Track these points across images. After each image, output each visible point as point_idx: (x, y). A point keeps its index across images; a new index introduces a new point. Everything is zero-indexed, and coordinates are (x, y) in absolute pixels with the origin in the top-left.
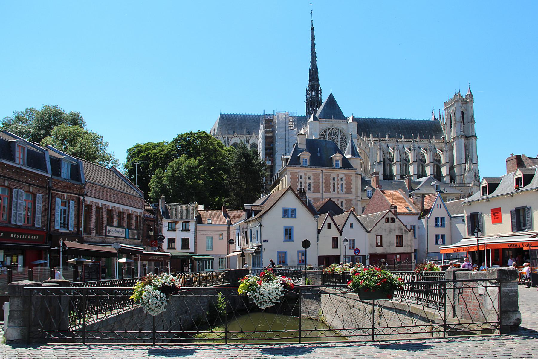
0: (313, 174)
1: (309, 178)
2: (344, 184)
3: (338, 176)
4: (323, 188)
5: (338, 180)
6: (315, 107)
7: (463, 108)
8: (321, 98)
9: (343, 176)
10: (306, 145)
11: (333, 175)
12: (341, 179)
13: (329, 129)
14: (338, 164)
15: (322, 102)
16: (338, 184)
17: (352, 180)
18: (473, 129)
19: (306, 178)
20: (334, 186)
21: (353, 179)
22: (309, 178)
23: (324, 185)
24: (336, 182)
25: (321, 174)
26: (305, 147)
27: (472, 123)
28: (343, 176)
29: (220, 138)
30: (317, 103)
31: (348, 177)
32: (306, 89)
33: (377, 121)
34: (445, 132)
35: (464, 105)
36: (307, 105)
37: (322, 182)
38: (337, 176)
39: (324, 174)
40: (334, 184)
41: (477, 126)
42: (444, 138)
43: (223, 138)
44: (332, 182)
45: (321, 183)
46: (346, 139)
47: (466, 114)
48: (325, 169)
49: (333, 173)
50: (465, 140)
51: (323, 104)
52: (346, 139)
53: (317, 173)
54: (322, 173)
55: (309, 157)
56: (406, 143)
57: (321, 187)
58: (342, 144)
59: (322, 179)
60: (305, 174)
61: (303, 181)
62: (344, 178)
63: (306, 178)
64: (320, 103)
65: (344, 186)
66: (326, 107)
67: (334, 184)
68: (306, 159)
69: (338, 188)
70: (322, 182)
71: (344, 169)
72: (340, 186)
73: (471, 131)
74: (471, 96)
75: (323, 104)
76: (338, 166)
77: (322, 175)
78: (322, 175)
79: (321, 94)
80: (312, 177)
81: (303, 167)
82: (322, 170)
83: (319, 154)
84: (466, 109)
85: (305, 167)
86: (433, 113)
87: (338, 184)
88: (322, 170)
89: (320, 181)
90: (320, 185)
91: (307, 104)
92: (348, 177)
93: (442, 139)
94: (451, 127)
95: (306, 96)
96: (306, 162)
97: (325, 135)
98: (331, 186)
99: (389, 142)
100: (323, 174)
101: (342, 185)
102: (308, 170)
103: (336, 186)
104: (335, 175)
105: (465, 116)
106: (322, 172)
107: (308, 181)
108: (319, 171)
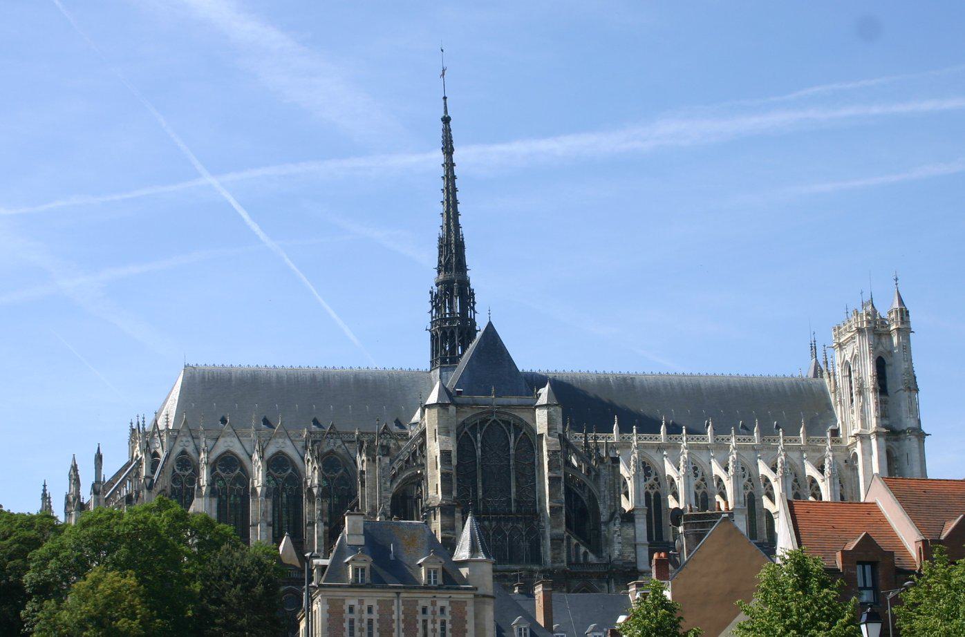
0: (379, 602)
1: (370, 610)
2: (448, 622)
3: (433, 604)
4: (401, 630)
5: (434, 613)
9: (445, 603)
10: (363, 538)
11: (422, 603)
12: (442, 610)
14: (435, 577)
16: (434, 622)
17: (466, 613)
18: (914, 410)
19: (361, 612)
20: (425, 627)
21: (470, 610)
22: (370, 610)
23: (402, 626)
24: (429, 616)
25: (396, 602)
26: (361, 540)
28: (445, 603)
31: (458, 607)
33: (637, 382)
37: (398, 619)
38: (432, 605)
39: (402, 600)
40: (425, 621)
41: (924, 398)
44: (420, 618)
45: (396, 622)
47: (891, 365)
48: (403, 590)
49: (424, 600)
50: (887, 440)
51: (479, 335)
53: (388, 599)
54: (398, 600)
55: (367, 565)
57: (396, 630)
59: (397, 613)
60: (361, 602)
61: (355, 616)
62: (448, 609)
63: (361, 612)
64: (469, 333)
65: (449, 626)
66: (474, 363)
67: (425, 621)
68: (363, 570)
69: (434, 630)
70: (398, 619)
71: (448, 589)
72: (438, 626)
75: (479, 335)
76: (435, 582)
77: (398, 603)
78: (398, 603)
80: (376, 608)
81: (356, 587)
82: (398, 594)
83: (392, 557)
85: (361, 587)
87: (434, 622)
88: (398, 594)
89: (395, 617)
90: (395, 626)
91: (432, 336)
92: (458, 607)
94: (852, 401)
96: (363, 575)
98: (420, 626)
100: (400, 601)
101: (443, 623)
102: (365, 594)
103: (430, 626)
104: (427, 603)
105: (889, 370)
106: (398, 596)
107: (366, 616)
108: (390, 595)
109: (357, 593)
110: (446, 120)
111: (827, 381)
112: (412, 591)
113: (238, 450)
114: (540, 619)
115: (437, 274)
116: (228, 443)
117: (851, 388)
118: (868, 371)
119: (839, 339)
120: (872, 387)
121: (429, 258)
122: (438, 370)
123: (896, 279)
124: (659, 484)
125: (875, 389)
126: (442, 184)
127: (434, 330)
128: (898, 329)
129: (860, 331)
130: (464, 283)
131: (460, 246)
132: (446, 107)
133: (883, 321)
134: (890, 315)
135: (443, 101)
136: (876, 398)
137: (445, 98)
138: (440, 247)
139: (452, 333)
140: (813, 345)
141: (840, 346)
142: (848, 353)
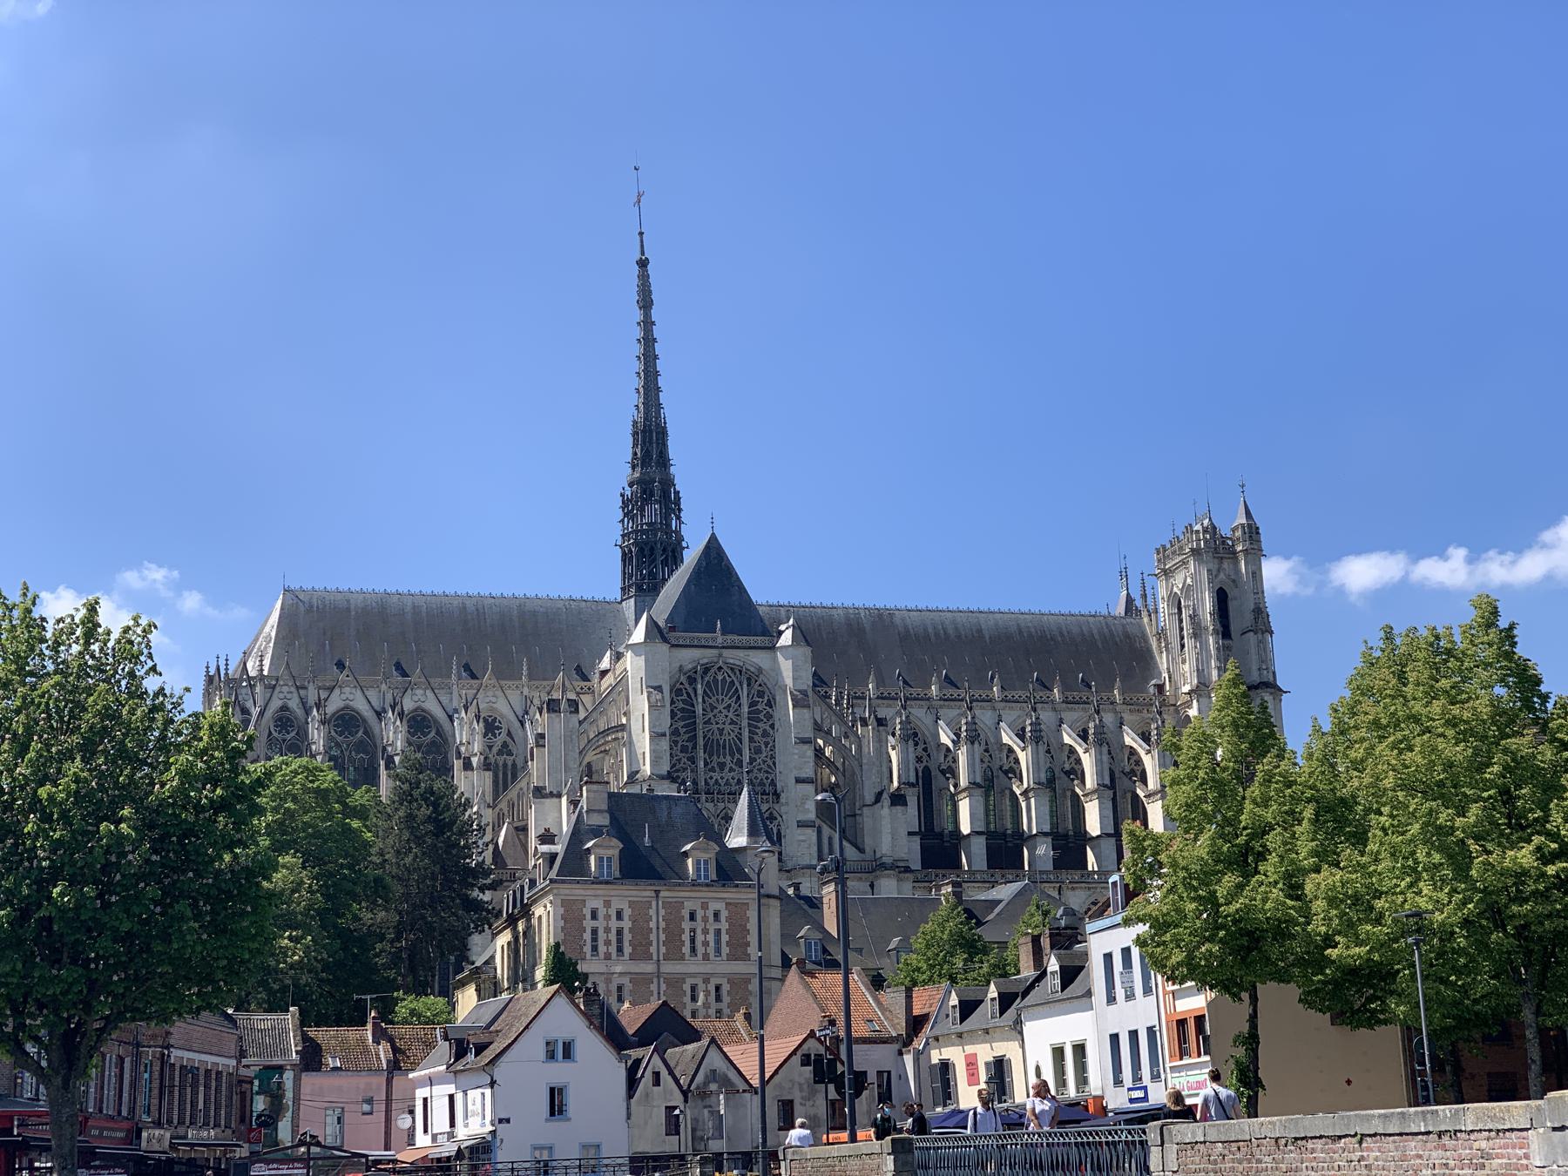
6: (655, 567)
7: (1222, 576)
8: (678, 532)
13: (706, 670)
15: (684, 544)
27: (1260, 636)
29: (285, 689)
30: (664, 550)
32: (622, 495)
33: (897, 620)
34: (1161, 658)
35: (1225, 565)
36: (626, 558)
42: (1160, 688)
43: (298, 688)
46: (771, 707)
47: (1235, 599)
52: (771, 707)
56: (1011, 708)
58: (756, 727)
73: (1255, 667)
74: (1252, 532)
79: (679, 518)
84: (1234, 581)
86: (1124, 574)
93: (1152, 690)
94: (1183, 646)
95: (622, 521)
97: (693, 695)
99: (941, 707)
105: (1232, 605)
109: (602, 890)
110: (643, 264)
111: (1146, 620)
112: (677, 888)
113: (360, 705)
114: (831, 925)
115: (630, 470)
116: (350, 697)
117: (1181, 629)
118: (1208, 604)
119: (1165, 565)
120: (1212, 628)
121: (623, 448)
122: (632, 600)
123: (1243, 486)
124: (929, 755)
125: (1215, 632)
126: (638, 349)
127: (627, 546)
128: (1245, 551)
129: (1195, 552)
130: (668, 483)
131: (662, 433)
132: (642, 246)
133: (1224, 540)
134: (1233, 531)
135: (638, 237)
136: (1217, 643)
137: (641, 234)
138: (635, 434)
139: (652, 549)
140: (1124, 574)
141: (1167, 573)
142: (1178, 581)
